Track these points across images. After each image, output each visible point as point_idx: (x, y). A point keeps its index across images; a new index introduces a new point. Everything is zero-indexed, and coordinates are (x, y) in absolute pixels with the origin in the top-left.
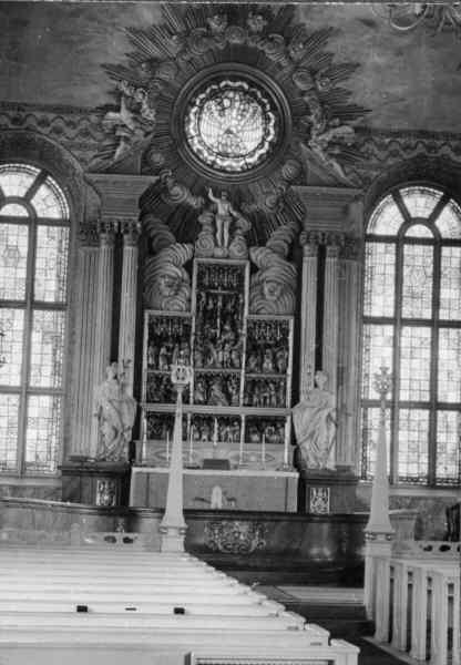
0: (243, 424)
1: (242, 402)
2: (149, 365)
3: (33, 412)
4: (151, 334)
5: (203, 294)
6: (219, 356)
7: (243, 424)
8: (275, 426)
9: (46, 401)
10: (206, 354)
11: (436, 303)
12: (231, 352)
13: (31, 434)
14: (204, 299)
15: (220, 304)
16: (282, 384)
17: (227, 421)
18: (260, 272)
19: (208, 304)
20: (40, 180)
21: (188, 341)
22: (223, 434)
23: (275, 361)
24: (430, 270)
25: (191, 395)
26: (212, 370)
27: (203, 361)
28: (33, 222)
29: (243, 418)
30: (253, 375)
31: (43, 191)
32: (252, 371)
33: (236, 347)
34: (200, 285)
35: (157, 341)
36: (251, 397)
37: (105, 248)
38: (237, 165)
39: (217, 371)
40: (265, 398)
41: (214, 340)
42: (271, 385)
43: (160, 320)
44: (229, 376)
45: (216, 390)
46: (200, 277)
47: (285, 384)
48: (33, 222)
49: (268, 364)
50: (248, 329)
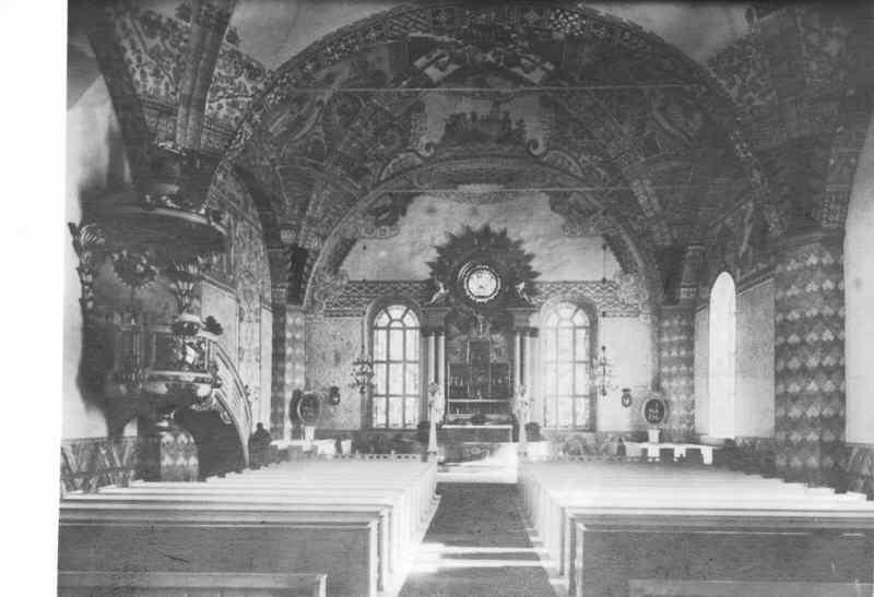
3: (407, 403)
9: (413, 399)
11: (574, 353)
13: (407, 412)
20: (406, 312)
24: (571, 339)
28: (404, 328)
31: (408, 316)
37: (432, 338)
38: (485, 300)
48: (404, 328)
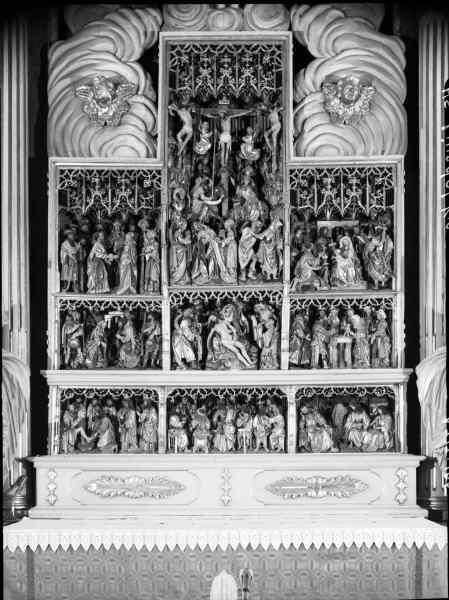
0: (292, 410)
1: (285, 357)
2: (63, 284)
4: (67, 216)
5: (185, 116)
6: (227, 254)
7: (292, 410)
8: (368, 411)
10: (198, 253)
12: (256, 248)
14: (187, 129)
15: (226, 138)
16: (382, 314)
17: (250, 402)
18: (316, 64)
19: (197, 137)
21: (153, 225)
22: (245, 433)
23: (363, 262)
25: (166, 346)
26: (213, 289)
27: (190, 268)
29: (291, 395)
30: (309, 296)
32: (306, 288)
33: (268, 234)
34: (175, 98)
35: (83, 230)
36: (307, 346)
39: (222, 289)
40: (341, 348)
41: (215, 224)
42: (356, 319)
43: (83, 181)
44: (254, 301)
45: (225, 333)
46: (172, 81)
47: (389, 313)
49: (346, 267)
50: (293, 194)
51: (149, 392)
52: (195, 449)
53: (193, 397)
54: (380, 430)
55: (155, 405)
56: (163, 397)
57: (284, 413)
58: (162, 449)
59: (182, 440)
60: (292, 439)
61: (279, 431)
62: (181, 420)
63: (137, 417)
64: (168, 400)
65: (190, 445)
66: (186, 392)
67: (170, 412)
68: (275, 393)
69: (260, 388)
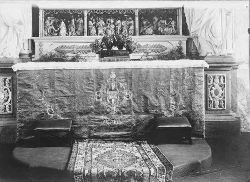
0: (137, 19)
7: (137, 19)
22: (119, 28)
51: (80, 11)
52: (99, 34)
53: (98, 13)
54: (172, 26)
55: (82, 17)
56: (86, 13)
57: (134, 19)
58: (86, 34)
59: (94, 30)
60: (137, 30)
61: (132, 27)
62: (93, 23)
63: (75, 22)
64: (88, 15)
65: (97, 33)
66: (95, 11)
67: (89, 19)
68: (130, 12)
69: (124, 10)
